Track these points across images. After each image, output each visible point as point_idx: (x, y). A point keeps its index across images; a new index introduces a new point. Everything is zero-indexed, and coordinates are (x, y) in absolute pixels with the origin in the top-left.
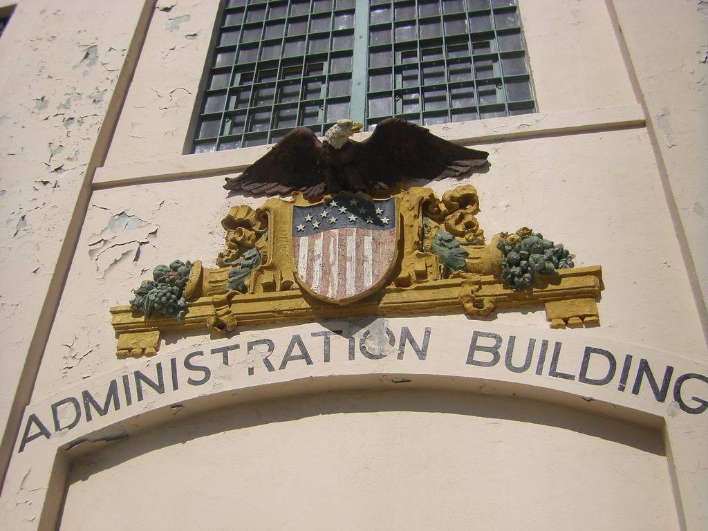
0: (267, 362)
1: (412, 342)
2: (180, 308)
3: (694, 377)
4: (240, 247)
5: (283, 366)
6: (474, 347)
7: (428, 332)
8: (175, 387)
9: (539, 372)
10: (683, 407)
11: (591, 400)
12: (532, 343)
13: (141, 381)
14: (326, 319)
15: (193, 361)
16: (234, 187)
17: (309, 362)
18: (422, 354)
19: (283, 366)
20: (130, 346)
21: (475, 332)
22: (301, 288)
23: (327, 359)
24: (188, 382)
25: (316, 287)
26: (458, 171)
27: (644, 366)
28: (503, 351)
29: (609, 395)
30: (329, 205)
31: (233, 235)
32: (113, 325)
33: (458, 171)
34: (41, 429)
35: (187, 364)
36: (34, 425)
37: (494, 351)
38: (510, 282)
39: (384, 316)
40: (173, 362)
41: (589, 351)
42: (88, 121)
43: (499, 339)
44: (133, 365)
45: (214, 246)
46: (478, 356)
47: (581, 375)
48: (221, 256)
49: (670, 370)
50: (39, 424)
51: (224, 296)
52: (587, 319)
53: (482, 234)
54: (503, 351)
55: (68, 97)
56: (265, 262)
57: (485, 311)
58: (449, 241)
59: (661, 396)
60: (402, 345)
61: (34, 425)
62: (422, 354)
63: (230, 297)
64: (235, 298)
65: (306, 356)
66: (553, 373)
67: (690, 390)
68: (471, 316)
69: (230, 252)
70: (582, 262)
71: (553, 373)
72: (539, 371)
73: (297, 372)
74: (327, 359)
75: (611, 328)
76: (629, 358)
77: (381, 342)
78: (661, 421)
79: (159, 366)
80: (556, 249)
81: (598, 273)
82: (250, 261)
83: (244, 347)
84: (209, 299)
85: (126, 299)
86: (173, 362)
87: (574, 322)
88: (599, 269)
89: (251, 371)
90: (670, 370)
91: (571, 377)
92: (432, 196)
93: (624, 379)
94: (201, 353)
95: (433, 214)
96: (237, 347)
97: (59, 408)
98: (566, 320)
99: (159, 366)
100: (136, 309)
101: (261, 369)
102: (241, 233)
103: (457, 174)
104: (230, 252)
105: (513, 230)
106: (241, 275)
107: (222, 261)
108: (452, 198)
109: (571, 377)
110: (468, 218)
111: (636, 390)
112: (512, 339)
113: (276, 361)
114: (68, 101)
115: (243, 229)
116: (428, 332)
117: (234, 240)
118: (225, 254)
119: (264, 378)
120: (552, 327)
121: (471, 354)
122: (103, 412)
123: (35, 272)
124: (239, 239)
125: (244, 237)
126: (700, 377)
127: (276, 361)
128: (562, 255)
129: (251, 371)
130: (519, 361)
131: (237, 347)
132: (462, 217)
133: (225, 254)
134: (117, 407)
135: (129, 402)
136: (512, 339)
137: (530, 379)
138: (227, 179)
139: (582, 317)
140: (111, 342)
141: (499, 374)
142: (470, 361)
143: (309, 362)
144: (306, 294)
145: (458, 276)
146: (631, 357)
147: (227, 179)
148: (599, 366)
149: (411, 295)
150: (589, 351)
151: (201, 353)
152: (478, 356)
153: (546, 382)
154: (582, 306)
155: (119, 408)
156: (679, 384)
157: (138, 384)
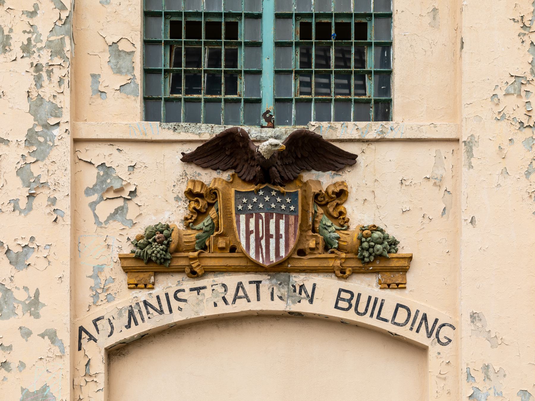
0: (224, 299)
1: (306, 292)
2: (168, 259)
3: (448, 326)
4: (200, 214)
5: (234, 300)
6: (339, 298)
7: (315, 285)
8: (171, 311)
9: (372, 315)
10: (439, 341)
11: (396, 334)
12: (370, 298)
13: (148, 307)
14: (256, 272)
15: (180, 295)
16: (187, 159)
17: (249, 301)
18: (311, 301)
19: (234, 300)
20: (136, 282)
21: (340, 289)
22: (242, 252)
23: (258, 300)
24: (179, 310)
25: (252, 254)
26: (337, 167)
27: (425, 318)
28: (354, 302)
29: (404, 332)
30: (258, 194)
31: (193, 205)
32: (122, 267)
33: (337, 167)
34: (89, 336)
35: (176, 297)
36: (83, 333)
37: (349, 301)
38: (362, 259)
39: (289, 272)
40: (167, 294)
41: (398, 306)
42: (58, 73)
43: (352, 295)
44: (142, 295)
45: (179, 209)
46: (342, 304)
47: (392, 321)
48: (186, 219)
49: (436, 321)
50: (87, 333)
51: (196, 254)
52: (400, 286)
53: (348, 221)
54: (354, 302)
55: (28, 36)
56: (217, 230)
57: (346, 276)
58: (330, 226)
59: (429, 335)
60: (300, 293)
61: (83, 333)
62: (311, 301)
63: (199, 254)
64: (202, 255)
65: (246, 296)
66: (378, 317)
67: (445, 332)
68: (339, 278)
69: (192, 216)
70: (403, 250)
71: (378, 317)
72: (372, 315)
73: (241, 306)
74: (258, 300)
75: (411, 292)
76: (418, 311)
77: (288, 291)
78: (428, 347)
79: (158, 297)
80: (390, 240)
81: (410, 258)
82: (208, 228)
83: (209, 289)
84: (186, 254)
85: (127, 250)
86: (167, 294)
87: (393, 287)
88: (411, 256)
89: (215, 305)
90: (436, 321)
91: (386, 320)
92: (321, 191)
93: (413, 324)
94: (183, 291)
95: (321, 201)
96: (204, 288)
97: (98, 323)
98: (389, 285)
99: (158, 297)
100: (138, 258)
101: (221, 303)
102: (197, 201)
103: (337, 169)
104: (192, 216)
105: (368, 222)
106: (205, 237)
107: (189, 223)
108: (333, 193)
109: (386, 320)
110: (341, 209)
111: (418, 331)
112: (359, 295)
113: (230, 298)
114: (29, 40)
115: (200, 200)
116: (315, 285)
117: (194, 208)
118: (189, 217)
119: (223, 309)
120: (381, 288)
121: (337, 303)
122: (128, 326)
123: (55, 221)
124: (198, 208)
125: (201, 207)
126: (451, 326)
127: (230, 299)
128: (394, 243)
129: (215, 305)
130: (361, 309)
131: (204, 288)
132: (338, 205)
133: (189, 217)
134: (136, 323)
135: (143, 319)
136: (359, 295)
137: (366, 320)
138: (183, 154)
139: (398, 285)
140: (122, 279)
141: (350, 316)
142: (336, 307)
143: (249, 301)
144: (247, 258)
145: (332, 252)
146: (419, 311)
147: (183, 154)
148: (402, 315)
149: (305, 262)
150: (398, 306)
151: (183, 291)
152: (342, 304)
153: (374, 322)
154: (398, 278)
155: (138, 325)
156: (439, 329)
157: (146, 308)
